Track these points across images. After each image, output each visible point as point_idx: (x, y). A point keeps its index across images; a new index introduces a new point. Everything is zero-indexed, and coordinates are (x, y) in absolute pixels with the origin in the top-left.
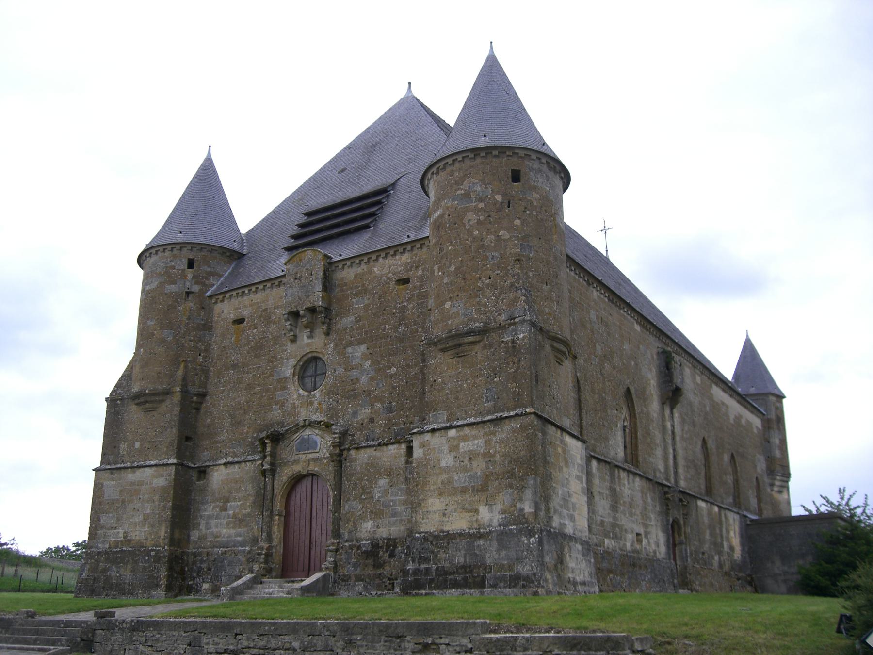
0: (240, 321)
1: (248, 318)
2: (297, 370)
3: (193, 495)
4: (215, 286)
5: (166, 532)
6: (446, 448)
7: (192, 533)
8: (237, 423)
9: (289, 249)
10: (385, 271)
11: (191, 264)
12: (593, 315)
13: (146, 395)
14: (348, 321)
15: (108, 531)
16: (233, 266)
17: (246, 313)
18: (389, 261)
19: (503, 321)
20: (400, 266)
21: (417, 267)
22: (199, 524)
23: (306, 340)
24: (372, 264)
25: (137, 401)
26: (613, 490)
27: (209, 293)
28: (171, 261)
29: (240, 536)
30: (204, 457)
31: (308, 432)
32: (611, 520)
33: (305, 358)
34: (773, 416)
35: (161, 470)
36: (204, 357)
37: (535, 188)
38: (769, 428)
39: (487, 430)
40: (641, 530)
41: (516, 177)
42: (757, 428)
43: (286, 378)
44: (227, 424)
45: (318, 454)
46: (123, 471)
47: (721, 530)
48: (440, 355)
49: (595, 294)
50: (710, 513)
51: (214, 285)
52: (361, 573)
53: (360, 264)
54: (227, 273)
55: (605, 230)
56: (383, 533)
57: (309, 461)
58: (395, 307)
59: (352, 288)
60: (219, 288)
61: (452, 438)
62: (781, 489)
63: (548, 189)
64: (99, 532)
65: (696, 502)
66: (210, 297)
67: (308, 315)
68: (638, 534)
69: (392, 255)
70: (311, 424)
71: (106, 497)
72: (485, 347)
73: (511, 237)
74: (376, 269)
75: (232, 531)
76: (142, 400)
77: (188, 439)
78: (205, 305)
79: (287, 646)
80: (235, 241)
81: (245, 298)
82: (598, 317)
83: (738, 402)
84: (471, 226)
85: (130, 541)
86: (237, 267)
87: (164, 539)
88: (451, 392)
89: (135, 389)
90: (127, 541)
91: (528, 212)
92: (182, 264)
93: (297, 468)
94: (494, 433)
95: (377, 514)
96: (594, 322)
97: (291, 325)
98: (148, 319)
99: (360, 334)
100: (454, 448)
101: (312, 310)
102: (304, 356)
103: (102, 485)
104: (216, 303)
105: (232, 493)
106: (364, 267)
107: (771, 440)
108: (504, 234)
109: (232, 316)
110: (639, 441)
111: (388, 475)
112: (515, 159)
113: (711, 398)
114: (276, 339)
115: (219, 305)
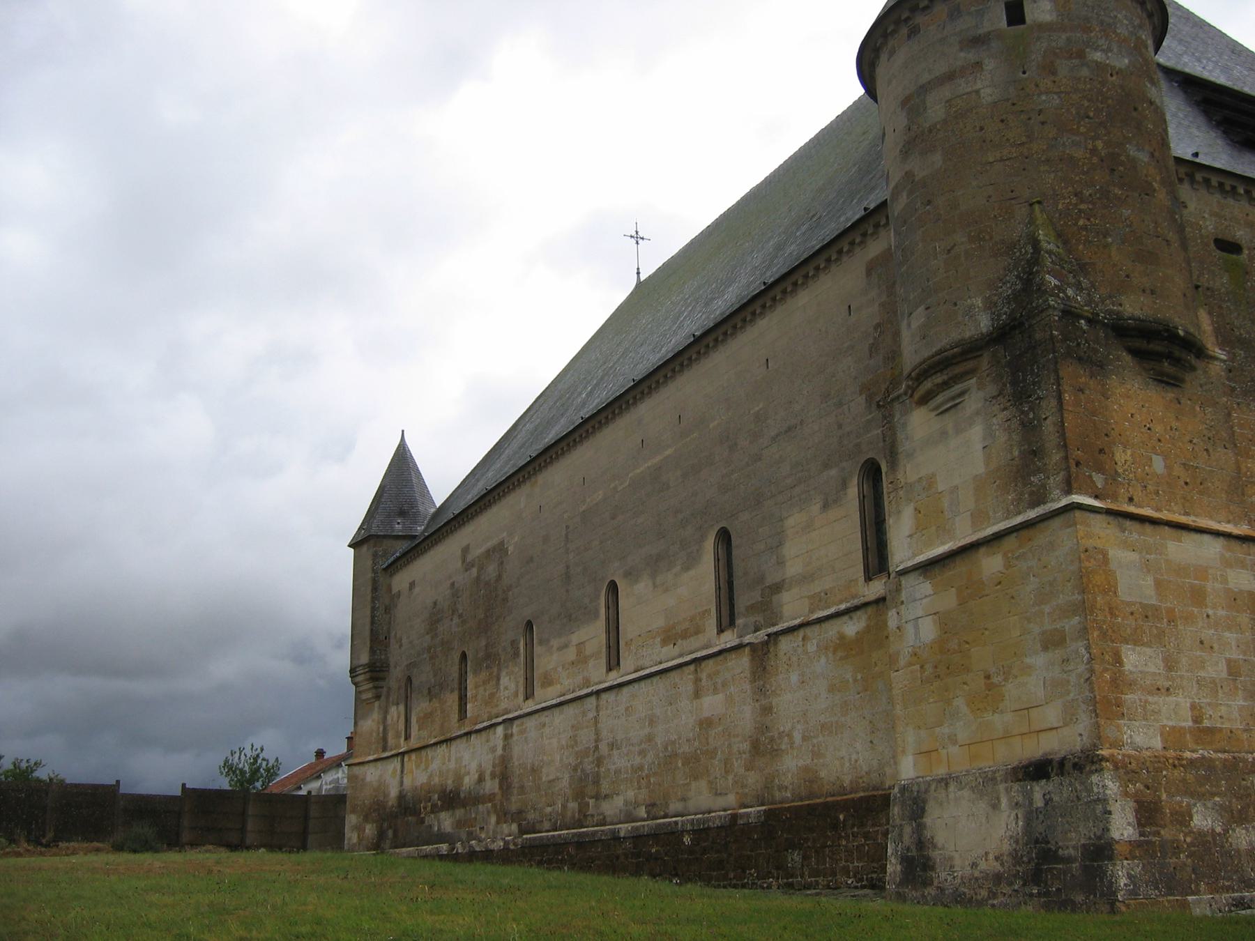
15: (1150, 699)
17: (1240, 234)
25: (1140, 344)
46: (1148, 528)
85: (1211, 731)
90: (1204, 734)
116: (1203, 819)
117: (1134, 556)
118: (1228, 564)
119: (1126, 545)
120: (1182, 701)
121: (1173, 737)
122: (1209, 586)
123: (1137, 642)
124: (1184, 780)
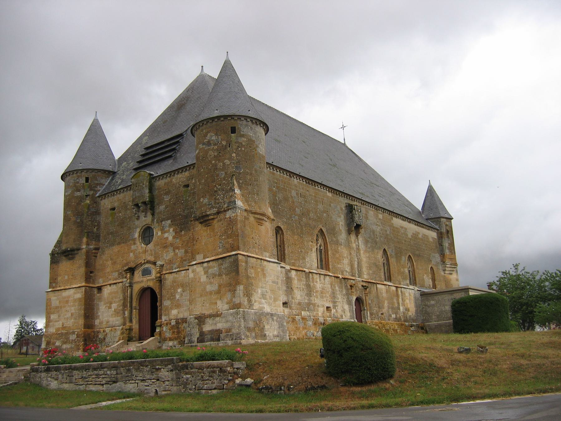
0: (113, 209)
1: (117, 207)
2: (141, 234)
3: (96, 301)
4: (101, 191)
5: (82, 322)
6: (203, 273)
7: (96, 321)
8: (114, 263)
9: (136, 169)
10: (178, 181)
11: (87, 180)
12: (294, 193)
13: (68, 251)
14: (162, 207)
16: (110, 178)
17: (116, 204)
18: (180, 176)
19: (226, 207)
20: (185, 178)
21: (192, 178)
22: (99, 316)
23: (144, 219)
24: (172, 177)
25: (65, 254)
26: (308, 286)
27: (97, 195)
28: (77, 179)
29: (118, 321)
30: (100, 282)
31: (147, 266)
32: (307, 301)
33: (144, 228)
34: (444, 230)
35: (78, 290)
36: (97, 229)
37: (243, 136)
38: (442, 237)
39: (220, 263)
40: (330, 305)
41: (233, 130)
42: (433, 238)
43: (135, 238)
44: (110, 263)
45: (151, 277)
46: (60, 291)
47: (398, 300)
48: (200, 225)
49: (295, 181)
50: (387, 291)
51: (100, 190)
52: (171, 337)
53: (166, 177)
54: (107, 183)
55: (343, 127)
56: (181, 316)
57: (148, 280)
58: (183, 200)
59: (163, 190)
60: (103, 192)
61: (205, 267)
62: (451, 272)
63: (252, 135)
64: (51, 324)
65: (376, 286)
66: (99, 197)
67: (143, 205)
68: (328, 308)
69: (181, 173)
70: (148, 262)
71: (53, 305)
72: (218, 221)
73: (230, 163)
74: (174, 180)
75: (114, 319)
76: (67, 254)
77: (91, 272)
78: (95, 201)
79: (105, 373)
80: (110, 165)
81: (115, 197)
82: (297, 194)
83: (416, 225)
84: (211, 158)
86: (112, 179)
87: (81, 325)
88: (205, 244)
89: (64, 248)
91: (239, 149)
92: (83, 181)
93: (144, 285)
94: (222, 264)
95: (178, 306)
96: (295, 197)
97: (136, 211)
98: (68, 211)
99: (168, 215)
100: (206, 272)
101: (144, 203)
102: (143, 226)
103: (50, 299)
104: (101, 200)
105: (113, 299)
106: (168, 179)
107: (443, 244)
108: (227, 162)
109: (110, 207)
110: (330, 257)
111: (182, 287)
112: (233, 121)
113: (391, 226)
114: (130, 218)
115: (103, 200)
116: (58, 343)
117: (56, 298)
118: (75, 293)
119: (55, 296)
120: (61, 323)
121: (58, 329)
122: (70, 299)
123: (54, 313)
124: (56, 337)
